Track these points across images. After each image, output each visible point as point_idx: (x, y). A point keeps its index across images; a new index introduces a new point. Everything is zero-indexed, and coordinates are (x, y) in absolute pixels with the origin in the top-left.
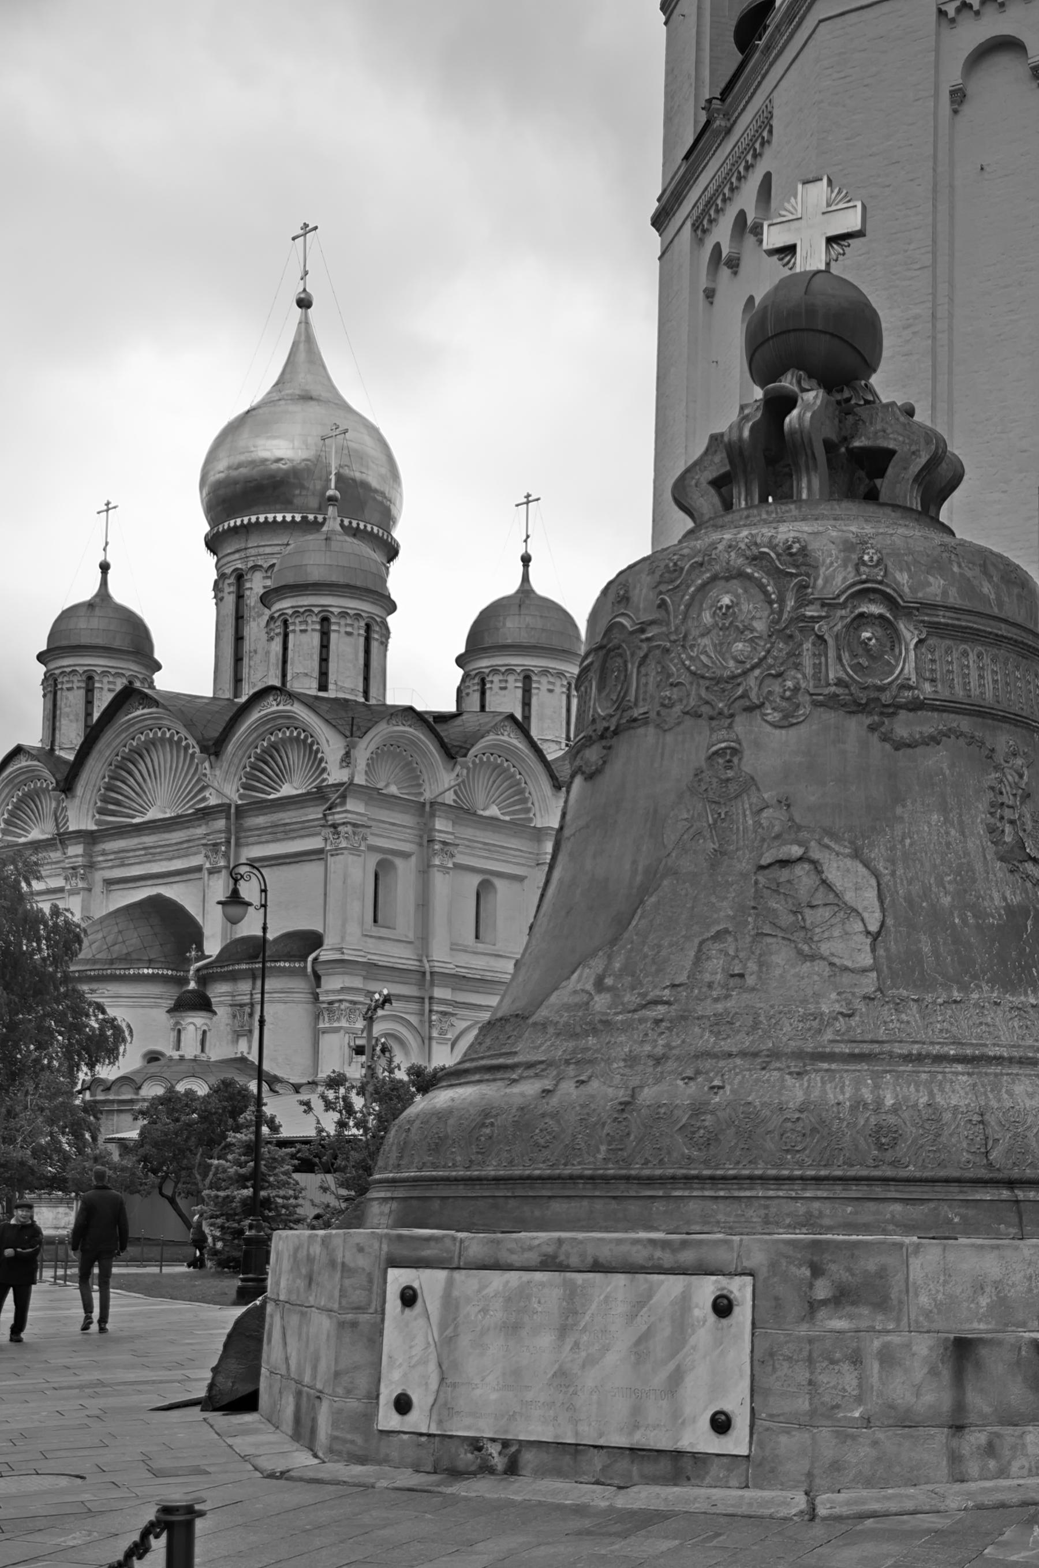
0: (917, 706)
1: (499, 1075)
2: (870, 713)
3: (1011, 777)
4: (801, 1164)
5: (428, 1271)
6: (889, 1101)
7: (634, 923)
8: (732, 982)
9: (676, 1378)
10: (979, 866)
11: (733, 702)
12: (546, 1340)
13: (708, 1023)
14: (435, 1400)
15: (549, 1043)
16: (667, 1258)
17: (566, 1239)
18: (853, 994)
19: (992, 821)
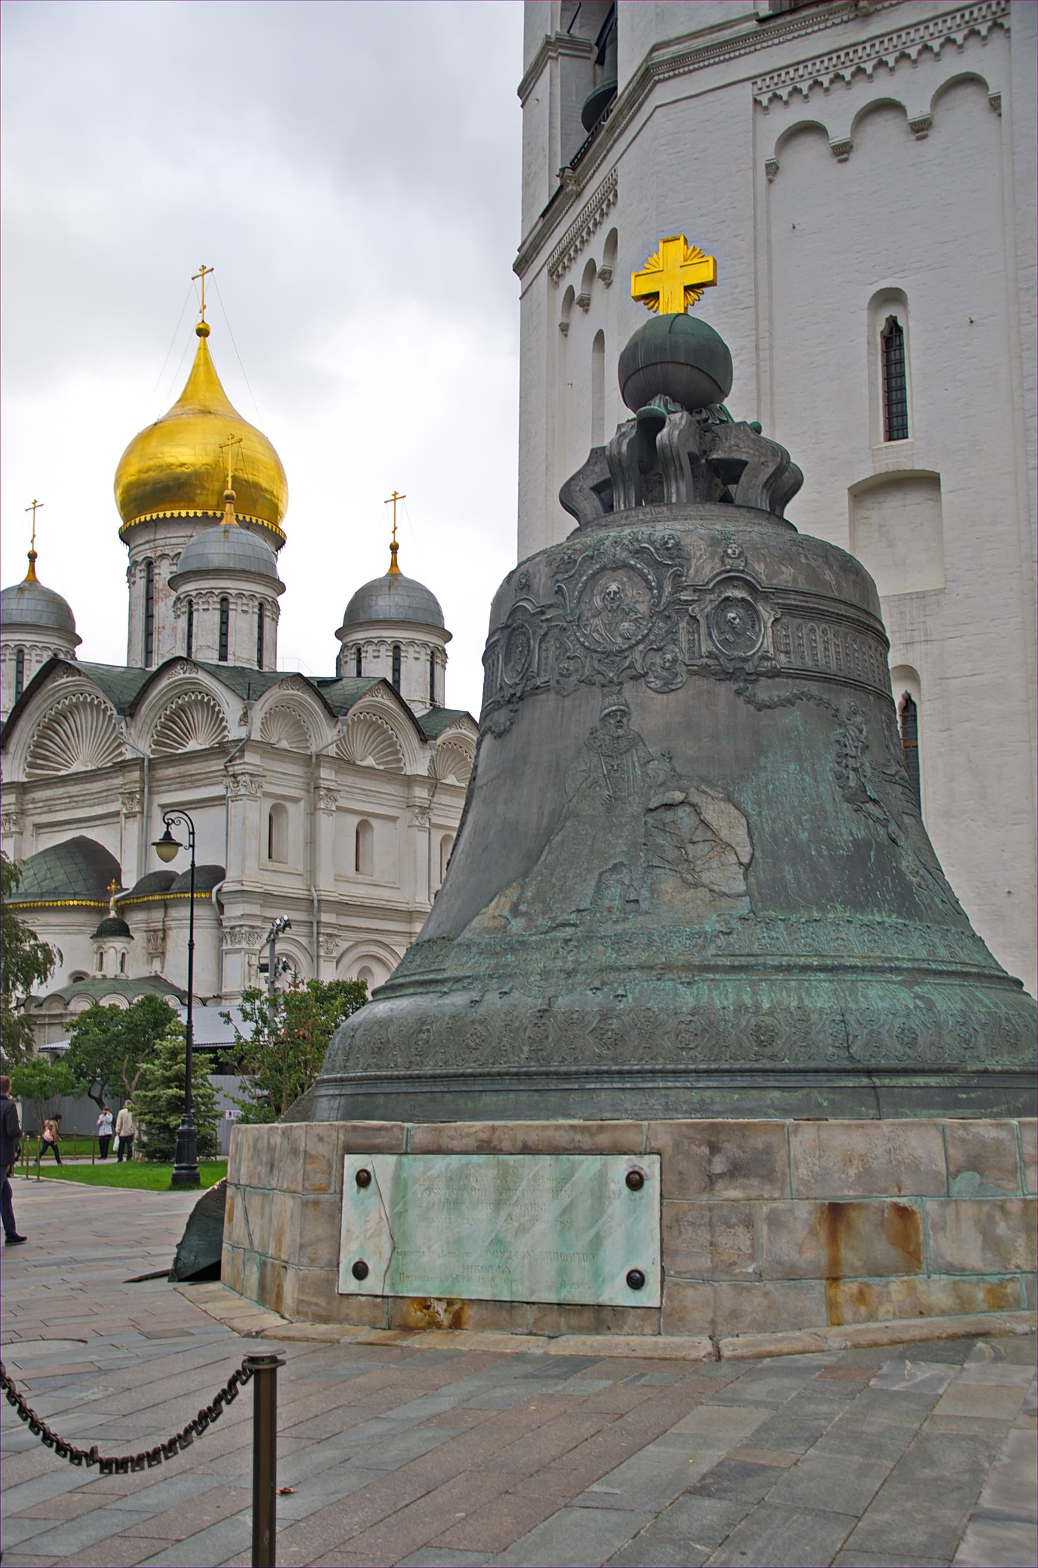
0: (775, 674)
1: (431, 989)
2: (736, 680)
3: (853, 732)
4: (694, 1059)
5: (380, 1156)
6: (766, 1005)
7: (542, 858)
8: (628, 907)
9: (596, 1244)
10: (829, 807)
12: (484, 1212)
13: (610, 942)
14: (388, 1267)
15: (473, 961)
16: (586, 1141)
17: (499, 1126)
18: (731, 915)
19: (839, 768)
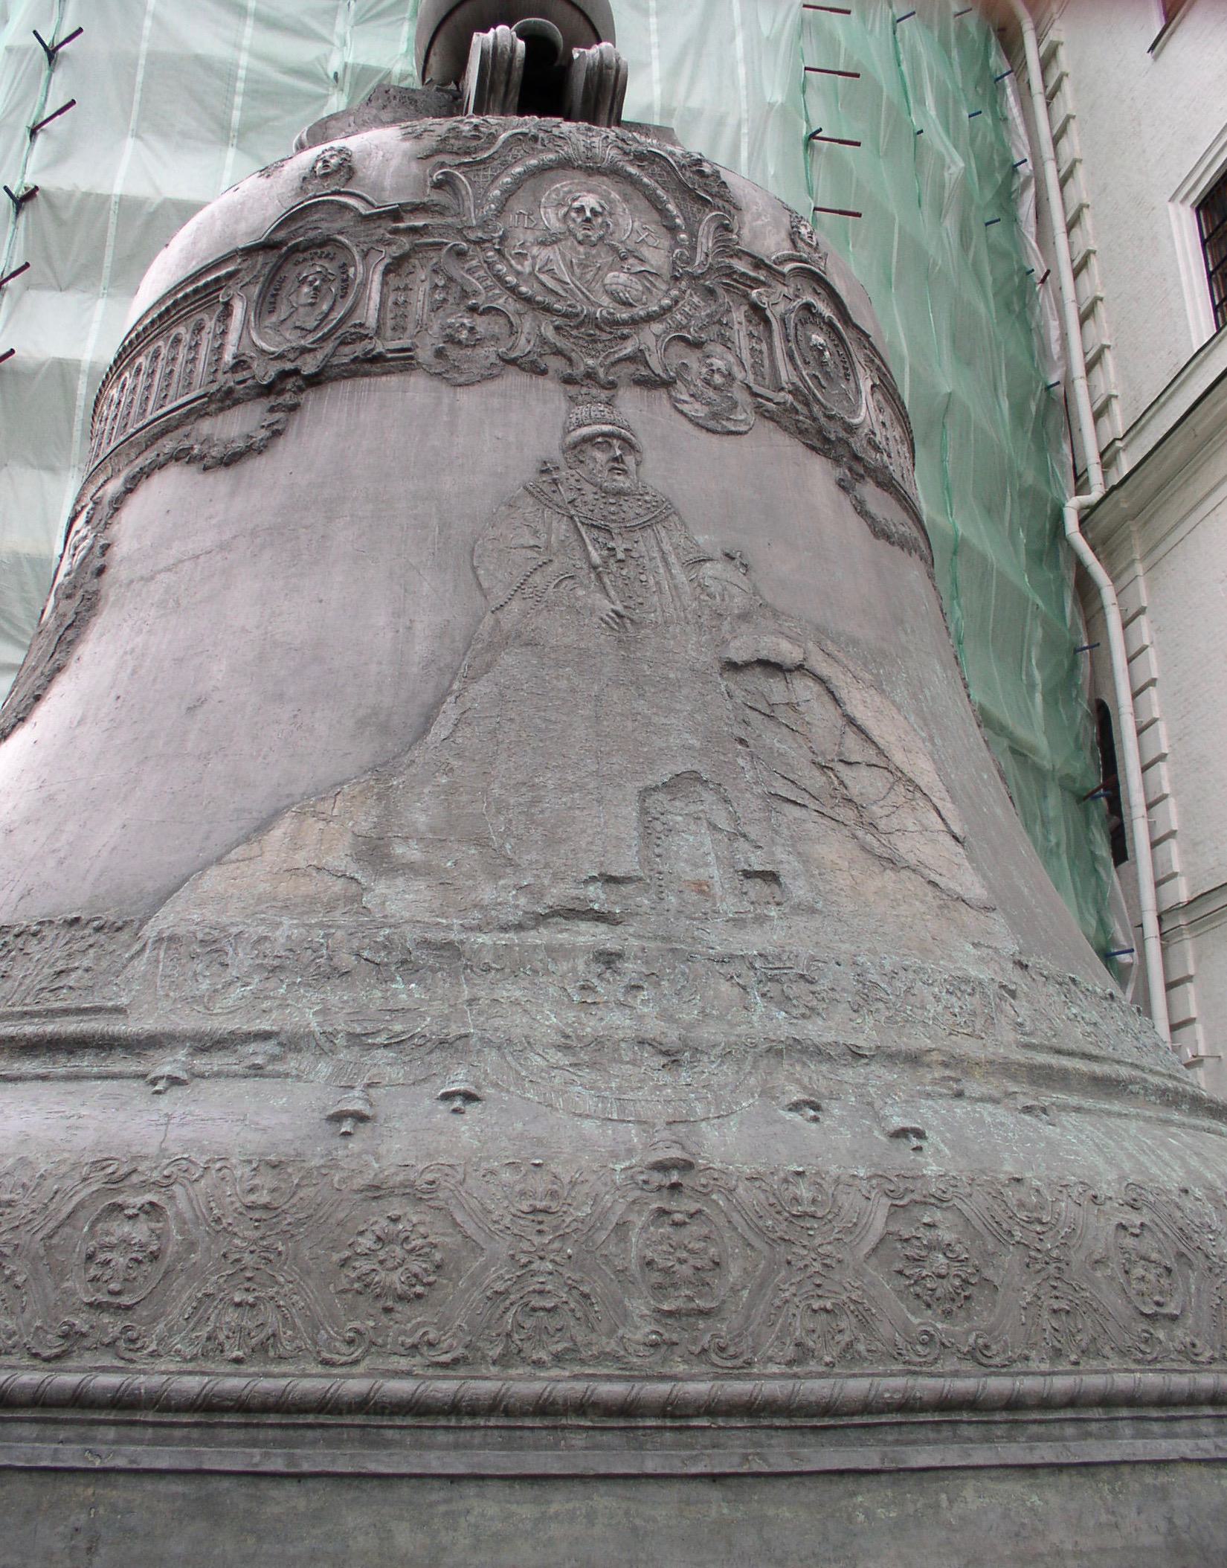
11: (614, 364)
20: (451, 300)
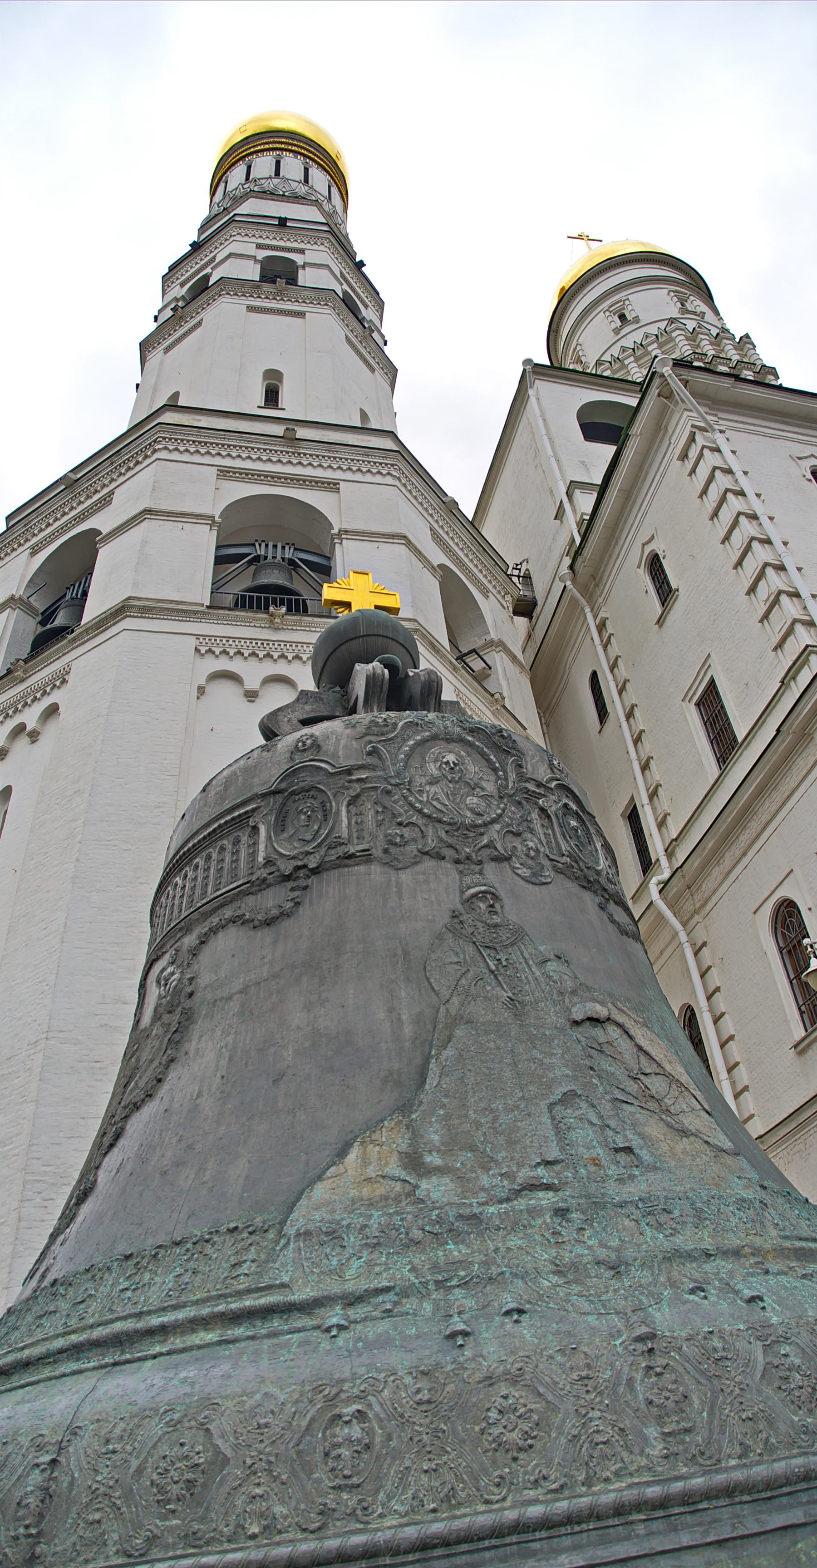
11: (479, 850)
20: (387, 820)
